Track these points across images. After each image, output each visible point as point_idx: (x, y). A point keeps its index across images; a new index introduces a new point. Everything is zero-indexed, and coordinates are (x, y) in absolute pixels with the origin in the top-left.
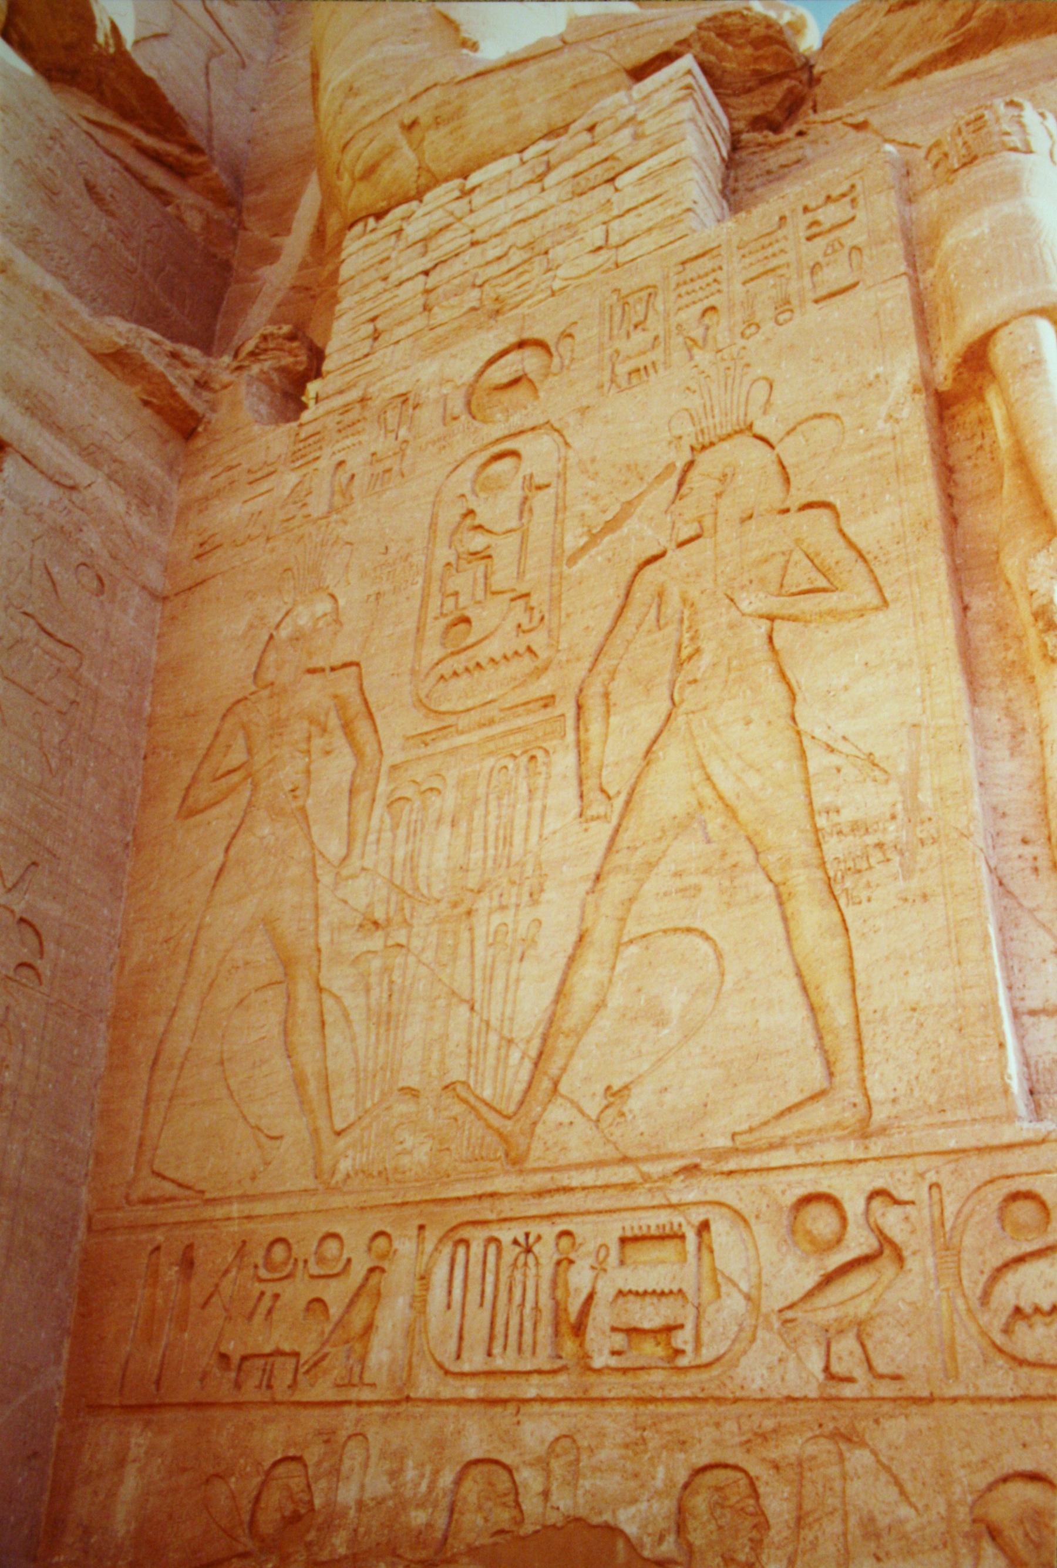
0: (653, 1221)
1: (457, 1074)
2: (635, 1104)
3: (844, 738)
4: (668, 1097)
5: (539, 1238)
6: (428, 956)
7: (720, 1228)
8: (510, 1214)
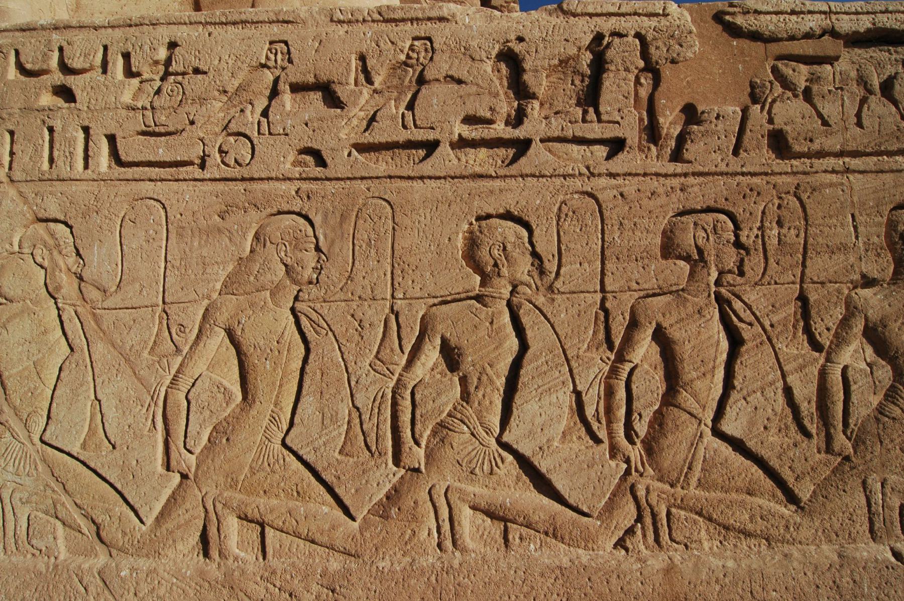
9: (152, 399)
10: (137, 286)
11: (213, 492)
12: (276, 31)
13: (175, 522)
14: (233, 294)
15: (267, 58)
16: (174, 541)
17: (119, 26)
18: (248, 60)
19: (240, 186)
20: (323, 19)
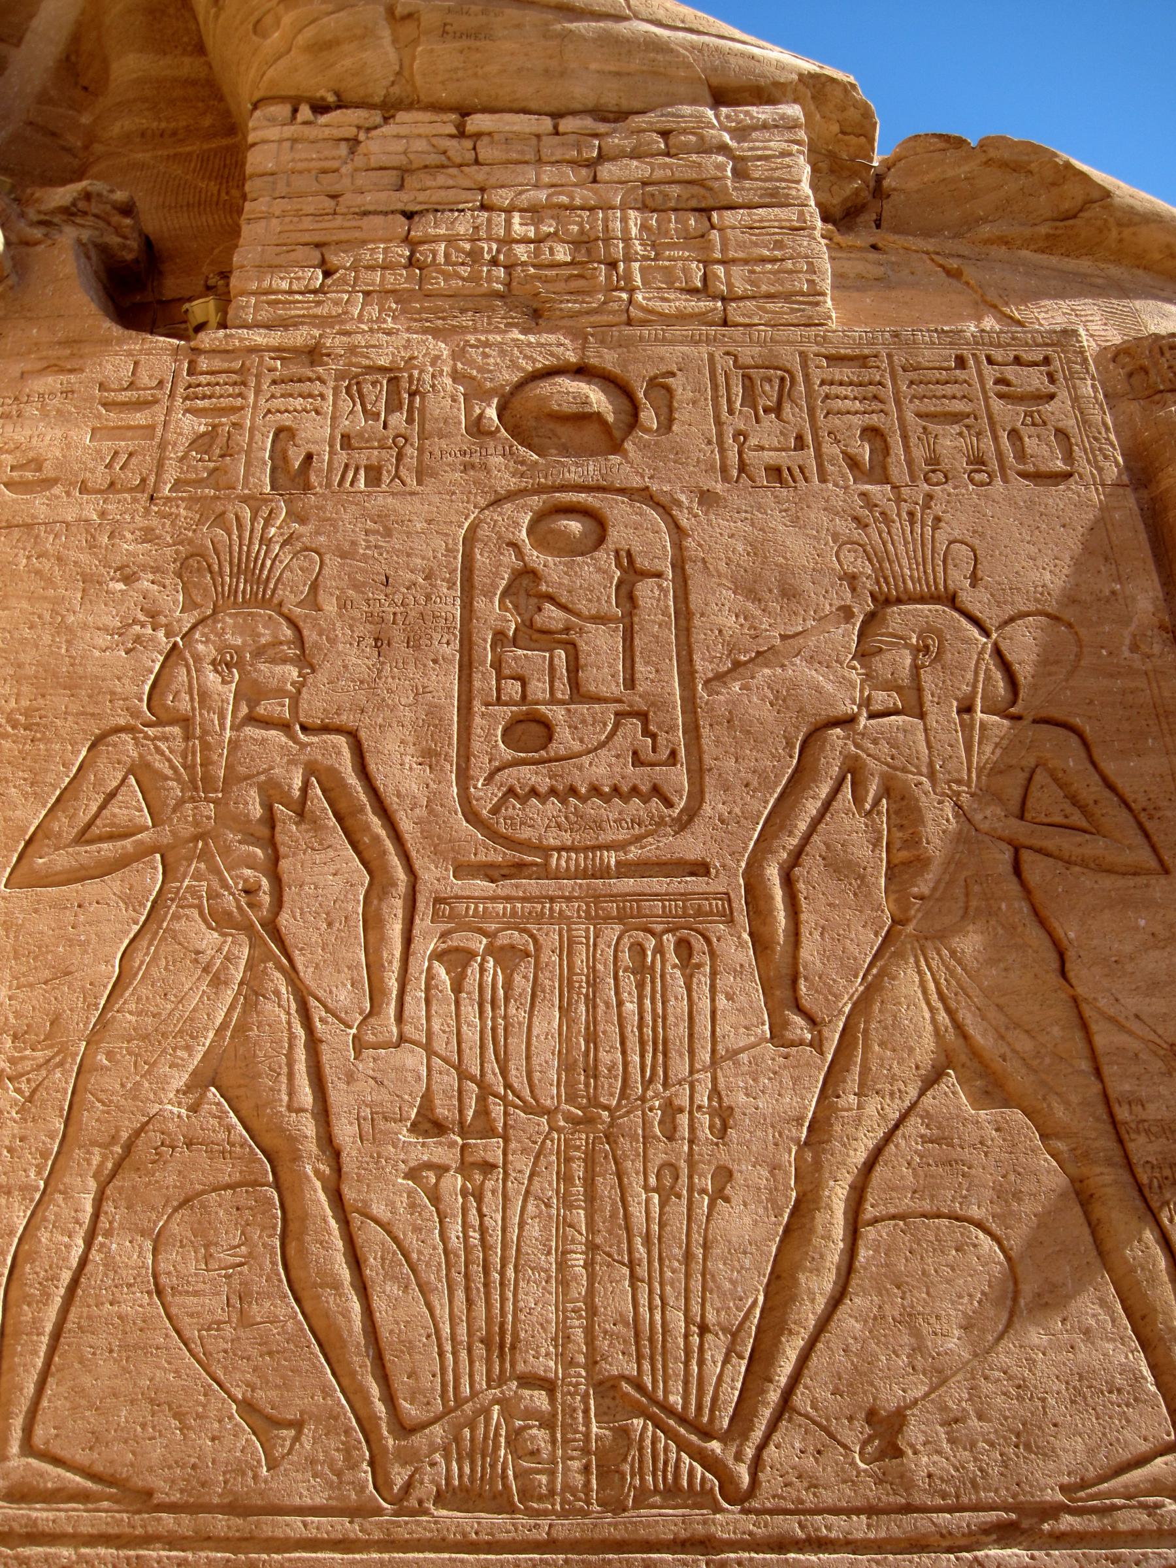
1: (621, 1364)
2: (914, 1432)
3: (1137, 1016)
6: (548, 1185)
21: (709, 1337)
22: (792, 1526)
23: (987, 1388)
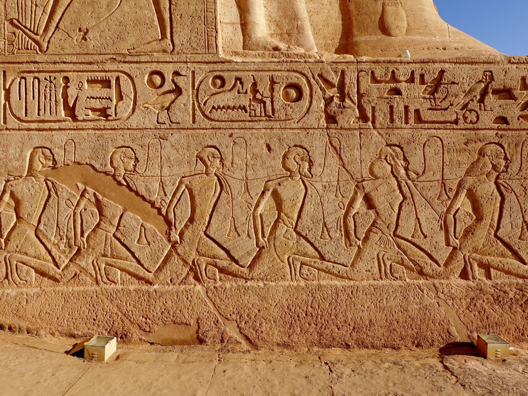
0: (100, 75)
2: (90, 35)
4: (103, 34)
5: (55, 78)
7: (123, 78)
8: (41, 69)
9: (440, 218)
10: (432, 173)
11: (468, 254)
12: (486, 66)
13: (453, 266)
14: (471, 176)
15: (483, 78)
16: (454, 273)
17: (418, 63)
18: (475, 79)
19: (473, 132)
20: (506, 62)
21: (37, 8)
22: (57, 59)
23: (111, 22)
